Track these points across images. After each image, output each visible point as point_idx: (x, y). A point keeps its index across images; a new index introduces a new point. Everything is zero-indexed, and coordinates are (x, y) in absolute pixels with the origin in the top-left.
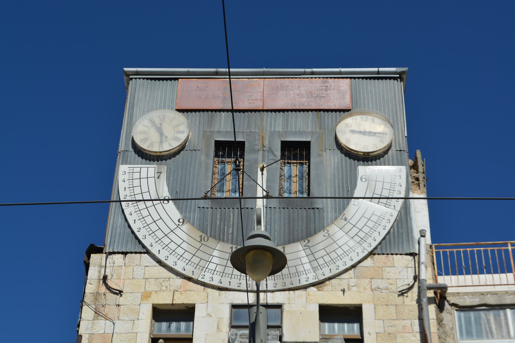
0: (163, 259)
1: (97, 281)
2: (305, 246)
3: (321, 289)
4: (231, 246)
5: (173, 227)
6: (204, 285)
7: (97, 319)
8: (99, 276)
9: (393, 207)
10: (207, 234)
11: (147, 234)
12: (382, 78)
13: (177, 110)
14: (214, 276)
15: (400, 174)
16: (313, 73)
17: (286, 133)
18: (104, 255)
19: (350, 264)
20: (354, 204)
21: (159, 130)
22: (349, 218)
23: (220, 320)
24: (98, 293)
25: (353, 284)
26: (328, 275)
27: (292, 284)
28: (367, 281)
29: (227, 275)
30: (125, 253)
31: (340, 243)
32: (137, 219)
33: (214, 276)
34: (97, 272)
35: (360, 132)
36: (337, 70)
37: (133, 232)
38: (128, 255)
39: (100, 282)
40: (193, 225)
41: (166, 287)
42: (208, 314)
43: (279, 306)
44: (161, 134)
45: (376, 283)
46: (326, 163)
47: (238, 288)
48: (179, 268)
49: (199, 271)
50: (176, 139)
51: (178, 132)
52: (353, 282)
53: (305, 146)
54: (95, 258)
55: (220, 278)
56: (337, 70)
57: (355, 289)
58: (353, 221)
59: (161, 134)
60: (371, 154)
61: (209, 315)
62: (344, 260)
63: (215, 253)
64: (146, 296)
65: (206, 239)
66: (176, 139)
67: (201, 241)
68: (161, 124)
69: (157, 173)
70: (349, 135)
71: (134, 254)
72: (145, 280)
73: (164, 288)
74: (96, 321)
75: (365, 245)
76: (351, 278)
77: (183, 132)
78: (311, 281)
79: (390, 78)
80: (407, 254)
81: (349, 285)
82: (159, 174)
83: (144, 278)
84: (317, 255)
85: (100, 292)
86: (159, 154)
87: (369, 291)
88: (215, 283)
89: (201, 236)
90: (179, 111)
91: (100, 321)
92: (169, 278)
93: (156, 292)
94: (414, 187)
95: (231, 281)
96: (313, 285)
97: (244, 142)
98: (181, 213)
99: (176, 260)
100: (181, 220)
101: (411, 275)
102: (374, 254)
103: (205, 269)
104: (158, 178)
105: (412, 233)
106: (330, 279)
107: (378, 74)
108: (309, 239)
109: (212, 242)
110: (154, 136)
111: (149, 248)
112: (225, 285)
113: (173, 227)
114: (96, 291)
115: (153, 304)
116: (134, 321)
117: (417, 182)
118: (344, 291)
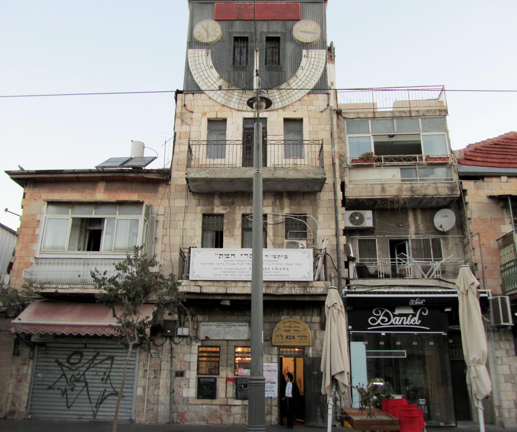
0: (211, 96)
5: (215, 80)
17: (268, 33)
18: (184, 95)
21: (207, 30)
22: (298, 76)
24: (182, 113)
26: (288, 104)
28: (306, 107)
30: (193, 94)
35: (304, 32)
37: (196, 83)
40: (225, 80)
44: (208, 33)
45: (310, 108)
46: (288, 49)
48: (219, 100)
50: (215, 36)
51: (216, 32)
52: (299, 107)
53: (277, 39)
54: (179, 96)
57: (300, 110)
58: (300, 78)
59: (208, 33)
61: (233, 123)
64: (204, 114)
66: (215, 36)
70: (299, 34)
77: (218, 32)
78: (280, 107)
84: (283, 94)
87: (306, 112)
90: (216, 20)
98: (219, 73)
101: (326, 105)
106: (288, 105)
110: (204, 34)
113: (215, 80)
118: (295, 111)
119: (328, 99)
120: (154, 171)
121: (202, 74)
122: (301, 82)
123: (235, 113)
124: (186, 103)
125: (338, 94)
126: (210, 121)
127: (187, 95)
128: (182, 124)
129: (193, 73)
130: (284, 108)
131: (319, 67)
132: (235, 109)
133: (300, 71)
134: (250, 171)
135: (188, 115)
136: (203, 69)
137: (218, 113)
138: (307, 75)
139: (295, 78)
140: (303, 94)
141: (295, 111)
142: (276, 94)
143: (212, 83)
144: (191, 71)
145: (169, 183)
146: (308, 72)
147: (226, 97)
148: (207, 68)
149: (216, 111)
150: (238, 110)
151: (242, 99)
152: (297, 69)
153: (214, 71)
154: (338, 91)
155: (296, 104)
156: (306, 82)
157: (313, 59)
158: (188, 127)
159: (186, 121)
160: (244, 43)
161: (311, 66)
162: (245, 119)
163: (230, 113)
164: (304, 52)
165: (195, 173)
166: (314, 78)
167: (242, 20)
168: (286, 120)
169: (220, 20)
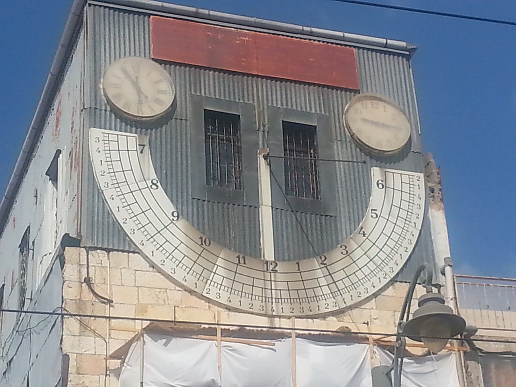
1: (78, 284)
2: (321, 264)
6: (209, 300)
8: (80, 278)
12: (390, 53)
13: (152, 59)
16: (311, 34)
20: (372, 216)
21: (136, 84)
22: (367, 233)
27: (311, 311)
30: (108, 251)
31: (361, 263)
34: (76, 271)
36: (341, 34)
38: (111, 253)
40: (188, 220)
41: (164, 300)
44: (139, 92)
47: (251, 310)
48: (179, 276)
49: (203, 284)
50: (158, 101)
52: (374, 313)
55: (229, 296)
56: (341, 34)
59: (139, 92)
60: (386, 153)
63: (220, 262)
66: (158, 101)
67: (202, 244)
68: (137, 77)
69: (140, 145)
71: (120, 252)
75: (387, 269)
76: (372, 308)
77: (163, 92)
79: (399, 55)
82: (142, 147)
83: (135, 286)
84: (336, 277)
86: (138, 119)
88: (223, 300)
89: (201, 238)
92: (166, 289)
96: (333, 314)
97: (239, 116)
100: (175, 214)
102: (396, 281)
103: (209, 282)
104: (142, 152)
106: (351, 308)
107: (385, 47)
108: (325, 254)
109: (213, 248)
112: (235, 304)
113: (167, 222)
114: (79, 297)
118: (367, 324)
121: (130, 198)
129: (107, 194)
132: (220, 305)
133: (369, 222)
136: (134, 187)
139: (362, 238)
140: (385, 282)
142: (319, 273)
143: (160, 227)
146: (390, 226)
148: (142, 185)
151: (238, 277)
156: (386, 249)
157: (398, 194)
160: (228, 132)
161: (395, 210)
164: (376, 173)
166: (405, 243)
167: (220, 71)
169: (171, 63)
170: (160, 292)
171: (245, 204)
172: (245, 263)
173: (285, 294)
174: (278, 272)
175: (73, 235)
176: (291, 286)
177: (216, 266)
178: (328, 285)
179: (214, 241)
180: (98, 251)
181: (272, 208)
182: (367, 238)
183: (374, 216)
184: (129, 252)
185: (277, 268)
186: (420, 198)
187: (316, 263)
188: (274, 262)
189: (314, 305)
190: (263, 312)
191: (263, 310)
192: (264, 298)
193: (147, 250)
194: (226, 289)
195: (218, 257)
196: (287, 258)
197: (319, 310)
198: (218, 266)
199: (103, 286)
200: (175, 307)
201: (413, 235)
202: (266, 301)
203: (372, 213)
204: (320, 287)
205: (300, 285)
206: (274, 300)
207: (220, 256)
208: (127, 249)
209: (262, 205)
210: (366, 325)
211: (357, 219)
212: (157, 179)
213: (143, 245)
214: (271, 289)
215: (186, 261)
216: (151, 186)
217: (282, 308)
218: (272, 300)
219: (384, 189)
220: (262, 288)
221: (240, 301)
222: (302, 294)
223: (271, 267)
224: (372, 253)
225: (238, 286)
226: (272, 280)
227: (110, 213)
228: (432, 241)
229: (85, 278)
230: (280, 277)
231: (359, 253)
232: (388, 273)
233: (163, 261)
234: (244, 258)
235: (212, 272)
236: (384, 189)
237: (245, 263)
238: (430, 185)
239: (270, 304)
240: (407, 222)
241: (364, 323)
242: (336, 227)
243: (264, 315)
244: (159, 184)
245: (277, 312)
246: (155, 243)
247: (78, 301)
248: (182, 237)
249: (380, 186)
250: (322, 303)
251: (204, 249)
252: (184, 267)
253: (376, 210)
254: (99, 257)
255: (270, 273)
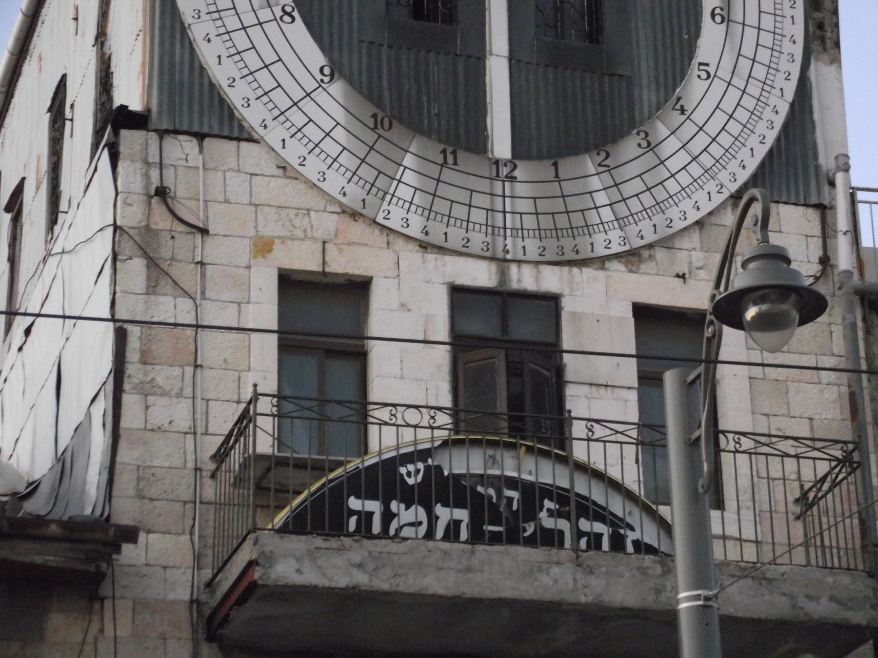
0: (295, 163)
2: (600, 165)
3: (634, 268)
4: (442, 147)
5: (310, 85)
7: (155, 293)
9: (779, 93)
10: (383, 110)
11: (252, 97)
14: (411, 216)
15: (792, 12)
19: (694, 216)
20: (699, 76)
22: (689, 108)
23: (428, 319)
24: (148, 227)
25: (700, 264)
26: (650, 238)
27: (577, 252)
29: (439, 217)
30: (201, 137)
31: (674, 164)
32: (224, 54)
33: (411, 216)
34: (139, 175)
38: (207, 142)
39: (150, 204)
40: (350, 81)
41: (305, 231)
42: (403, 305)
43: (552, 301)
47: (465, 250)
49: (377, 201)
54: (130, 139)
62: (683, 206)
63: (409, 160)
64: (263, 247)
65: (386, 126)
67: (376, 127)
72: (253, 208)
73: (299, 233)
74: (153, 297)
76: (694, 249)
78: (616, 249)
80: (806, 205)
81: (690, 263)
83: (251, 204)
84: (628, 189)
85: (154, 227)
88: (415, 230)
89: (374, 116)
91: (162, 299)
92: (308, 210)
93: (283, 239)
94: (816, 46)
95: (449, 230)
96: (617, 256)
99: (324, 167)
100: (327, 71)
103: (388, 197)
105: (816, 156)
106: (651, 246)
108: (608, 148)
109: (398, 133)
111: (261, 131)
113: (310, 85)
114: (143, 224)
115: (280, 269)
116: (239, 304)
117: (818, 32)
118: (683, 277)
119: (827, 232)
120: (54, 529)
122: (702, 141)
123: (411, 256)
124: (169, 182)
125: (863, 211)
126: (290, 283)
127: (169, 141)
128: (152, 288)
129: (198, 32)
130: (632, 257)
131: (781, 76)
132: (409, 238)
133: (695, 87)
134: (555, 570)
135: (185, 244)
137: (332, 252)
138: (728, 105)
139: (678, 118)
140: (718, 199)
141: (683, 277)
142: (595, 183)
143: (297, 94)
144: (188, 19)
145: (106, 589)
146: (733, 95)
147: (367, 173)
148: (265, 14)
149: (319, 234)
150: (424, 246)
151: (443, 190)
152: (683, 74)
153: (298, 31)
154: (860, 196)
155: (685, 243)
158: (185, 304)
159: (176, 271)
162: (461, 296)
163: (386, 258)
165: (299, 560)
168: (644, 314)
170: (296, 215)
171: (459, 53)
172: (455, 163)
173: (529, 222)
174: (518, 179)
175: (136, 105)
176: (543, 206)
177: (402, 168)
178: (610, 205)
179: (401, 121)
180: (182, 137)
181: (510, 60)
182: (688, 118)
183: (704, 75)
184: (239, 139)
185: (516, 173)
186: (794, 42)
187: (589, 164)
188: (510, 161)
189: (583, 242)
190: (488, 254)
191: (488, 250)
192: (490, 229)
193: (274, 135)
194: (420, 210)
195: (407, 151)
196: (534, 153)
197: (592, 251)
198: (405, 168)
199: (192, 204)
200: (324, 243)
201: (777, 112)
202: (493, 234)
203: (699, 70)
204: (596, 208)
205: (559, 205)
206: (508, 232)
207: (410, 150)
208: (236, 133)
209: (491, 54)
210: (681, 280)
211: (670, 81)
212: (293, 4)
213: (265, 127)
214: (504, 212)
215: (345, 158)
216: (281, 18)
217: (524, 247)
218: (505, 232)
219: (724, 24)
220: (488, 210)
221: (446, 234)
222: (562, 221)
223: (504, 171)
224: (697, 146)
225: (441, 206)
226: (507, 194)
227: (202, 69)
228: (813, 122)
229: (157, 189)
230: (521, 189)
231: (671, 145)
232: (726, 183)
233: (302, 159)
234: (454, 153)
235: (394, 179)
236: (724, 25)
237: (455, 163)
238: (817, 15)
239: (501, 239)
240: (766, 87)
241: (678, 276)
242: (630, 97)
243: (492, 259)
244: (296, 14)
245: (515, 253)
246: (288, 124)
247: (143, 230)
248: (340, 114)
249: (718, 19)
250: (599, 239)
251: (380, 136)
252: (342, 170)
253: (707, 65)
254: (181, 149)
255: (504, 181)
